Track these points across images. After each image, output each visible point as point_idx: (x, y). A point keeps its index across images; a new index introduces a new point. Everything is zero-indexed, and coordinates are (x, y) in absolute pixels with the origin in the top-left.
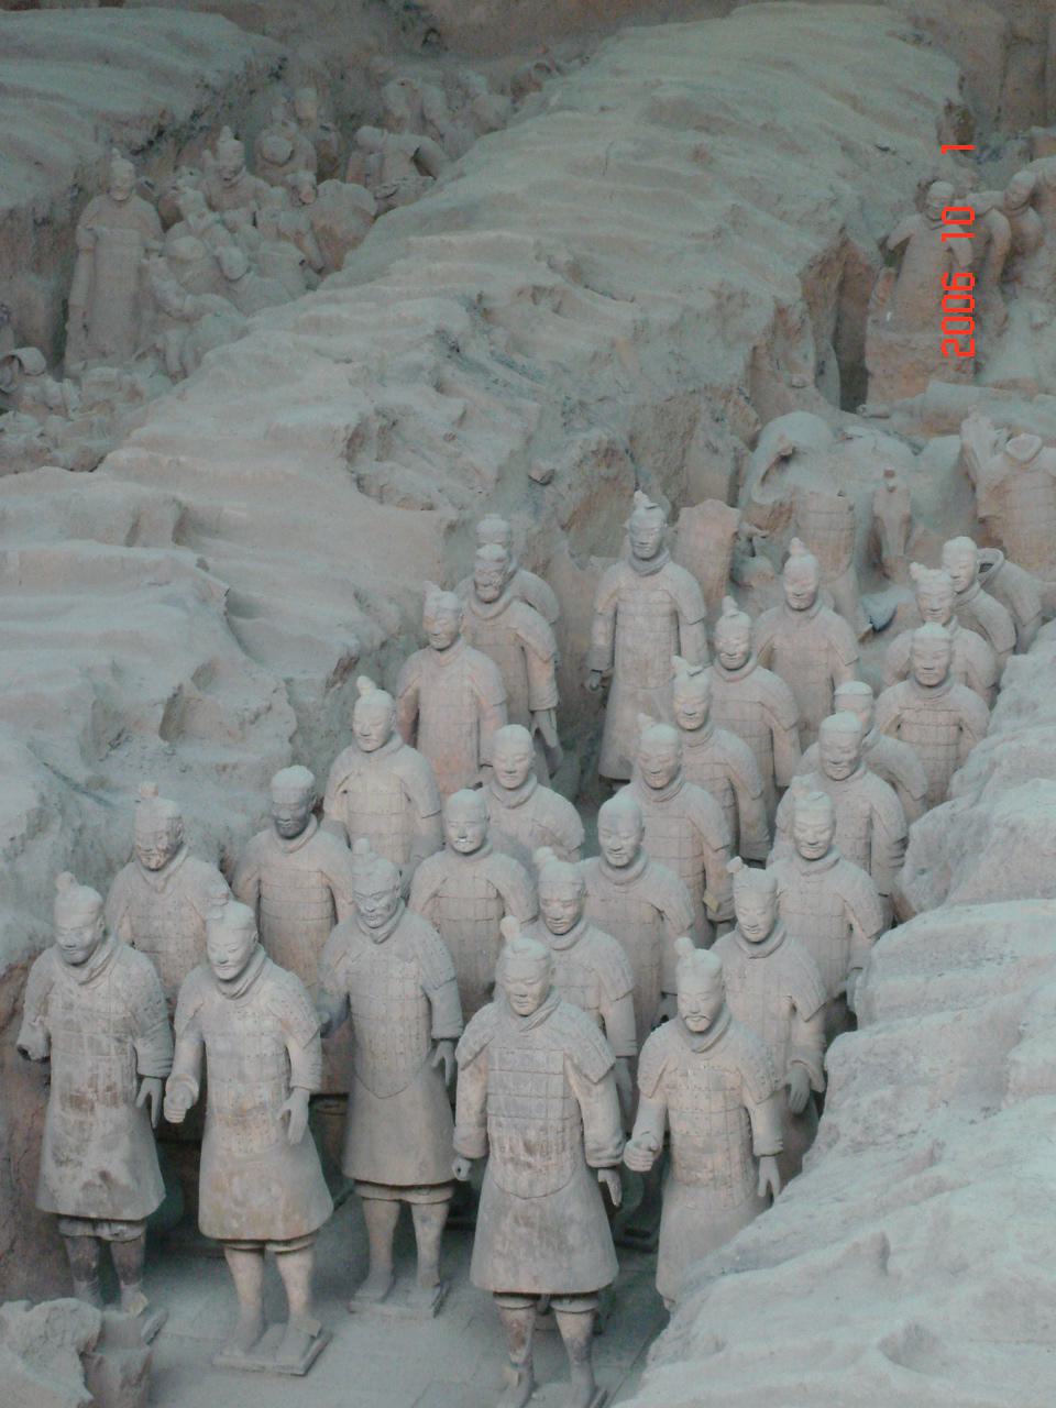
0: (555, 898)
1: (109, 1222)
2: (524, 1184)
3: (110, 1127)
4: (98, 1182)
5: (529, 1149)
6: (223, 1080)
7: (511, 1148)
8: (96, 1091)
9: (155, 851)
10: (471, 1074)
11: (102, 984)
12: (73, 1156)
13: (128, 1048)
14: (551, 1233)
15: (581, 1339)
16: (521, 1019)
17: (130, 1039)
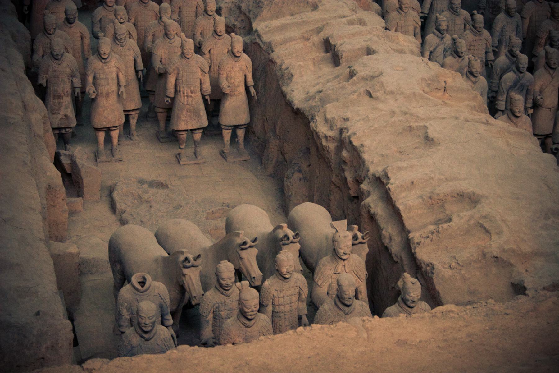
0: (172, 29)
1: (65, 128)
2: (190, 101)
3: (67, 102)
4: (64, 118)
5: (192, 92)
6: (103, 86)
7: (187, 93)
8: (64, 93)
9: (52, 29)
10: (173, 75)
11: (64, 64)
12: (57, 111)
13: (70, 80)
14: (196, 113)
15: (199, 139)
16: (187, 59)
17: (71, 78)
